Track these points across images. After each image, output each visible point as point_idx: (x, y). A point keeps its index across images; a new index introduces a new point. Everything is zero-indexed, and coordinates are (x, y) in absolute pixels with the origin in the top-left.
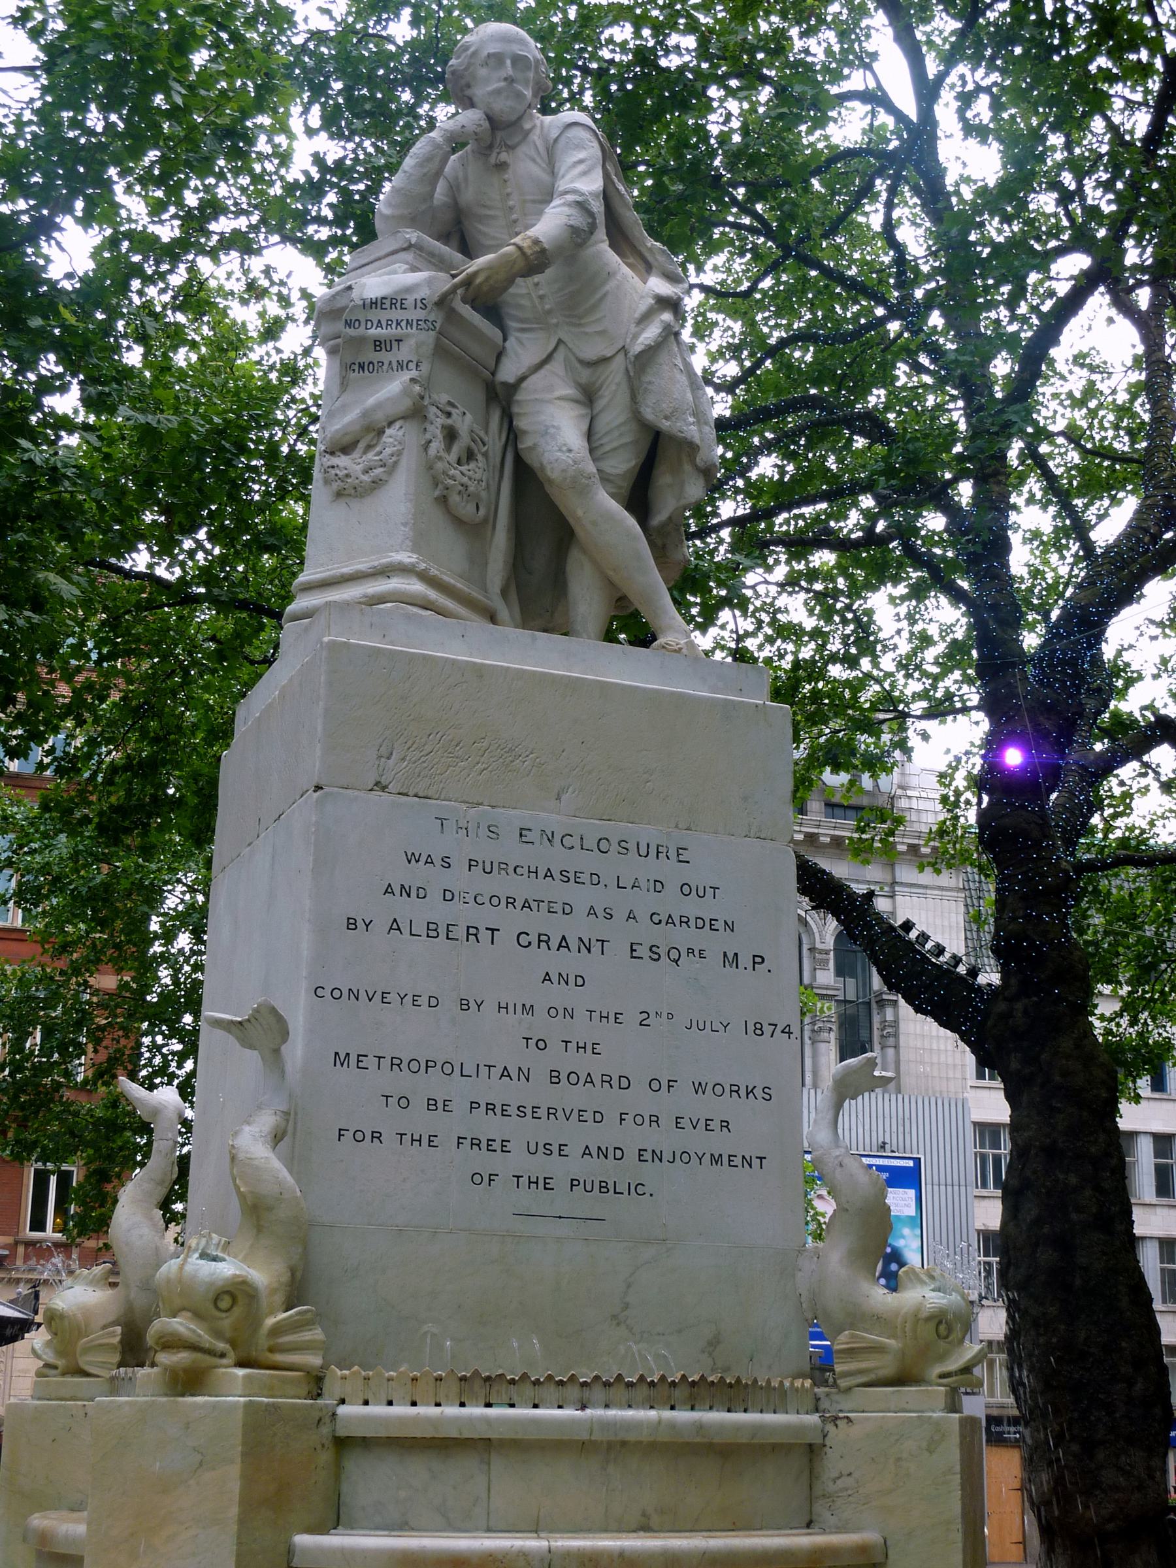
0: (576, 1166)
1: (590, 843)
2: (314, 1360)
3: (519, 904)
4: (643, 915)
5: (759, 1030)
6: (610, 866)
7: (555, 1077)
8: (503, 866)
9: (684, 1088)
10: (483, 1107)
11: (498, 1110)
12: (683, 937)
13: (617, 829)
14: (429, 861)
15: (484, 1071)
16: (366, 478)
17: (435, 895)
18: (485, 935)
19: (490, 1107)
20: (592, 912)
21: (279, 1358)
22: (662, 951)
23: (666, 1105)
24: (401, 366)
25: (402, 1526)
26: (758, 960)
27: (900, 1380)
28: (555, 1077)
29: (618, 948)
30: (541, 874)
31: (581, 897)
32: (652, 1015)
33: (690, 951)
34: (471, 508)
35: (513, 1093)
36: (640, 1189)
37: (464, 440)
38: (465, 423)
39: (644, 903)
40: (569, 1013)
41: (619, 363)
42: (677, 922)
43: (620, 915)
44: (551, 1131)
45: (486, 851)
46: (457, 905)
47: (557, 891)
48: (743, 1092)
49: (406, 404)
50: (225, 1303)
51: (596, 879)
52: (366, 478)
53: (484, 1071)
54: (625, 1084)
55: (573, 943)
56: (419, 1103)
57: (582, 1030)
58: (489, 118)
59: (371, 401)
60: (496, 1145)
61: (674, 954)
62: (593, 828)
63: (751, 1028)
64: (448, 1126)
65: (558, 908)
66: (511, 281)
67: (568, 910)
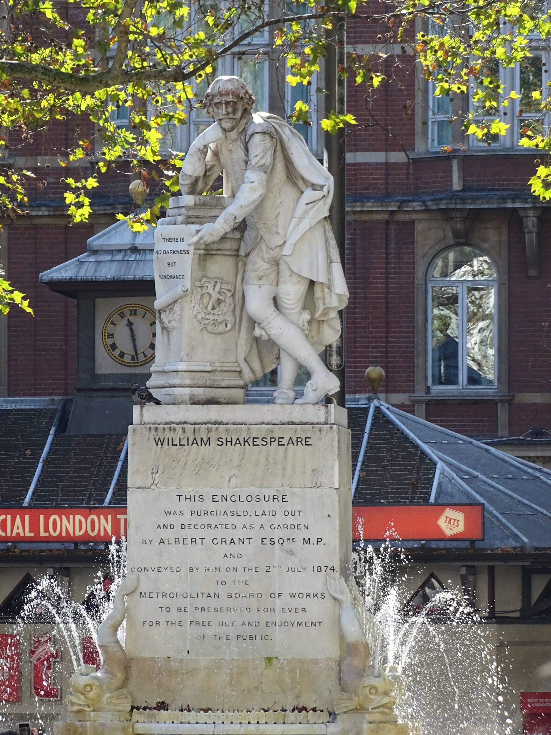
0: (239, 630)
3: (213, 527)
8: (206, 513)
9: (286, 597)
10: (200, 609)
11: (206, 610)
13: (255, 491)
15: (200, 595)
17: (178, 527)
19: (203, 609)
20: (245, 527)
22: (276, 540)
23: (279, 603)
26: (319, 540)
28: (230, 596)
30: (222, 513)
32: (271, 567)
33: (288, 539)
35: (213, 603)
36: (267, 638)
42: (282, 527)
43: (257, 527)
44: (227, 618)
45: (198, 506)
47: (230, 520)
48: (312, 596)
50: (88, 689)
53: (200, 595)
55: (236, 541)
56: (174, 610)
57: (241, 576)
60: (206, 624)
61: (281, 541)
63: (316, 569)
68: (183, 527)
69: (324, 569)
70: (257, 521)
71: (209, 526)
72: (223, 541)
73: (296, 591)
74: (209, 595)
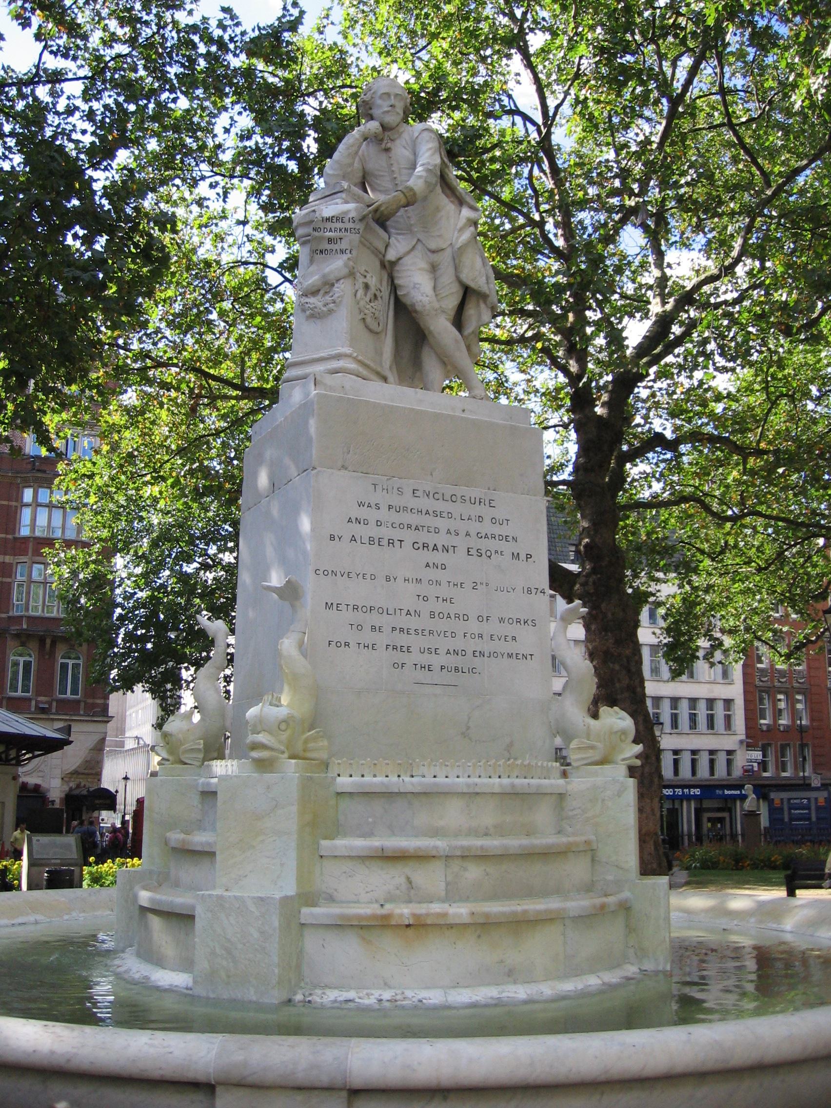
1: (447, 497)
2: (324, 755)
3: (413, 528)
4: (473, 533)
5: (529, 591)
6: (457, 509)
7: (432, 615)
8: (405, 509)
12: (493, 545)
13: (461, 490)
14: (369, 506)
16: (325, 309)
18: (397, 544)
19: (402, 630)
20: (449, 532)
21: (308, 755)
22: (483, 552)
24: (342, 252)
25: (369, 834)
26: (529, 556)
27: (602, 762)
28: (432, 615)
29: (462, 551)
31: (442, 524)
33: (496, 552)
34: (376, 324)
35: (413, 623)
37: (373, 290)
38: (373, 281)
39: (474, 527)
40: (438, 583)
41: (449, 252)
43: (462, 533)
45: (396, 500)
46: (383, 529)
49: (345, 271)
51: (450, 515)
52: (325, 309)
54: (466, 618)
55: (440, 547)
56: (367, 628)
57: (444, 591)
58: (382, 125)
59: (327, 270)
60: (404, 649)
61: (488, 553)
62: (449, 490)
64: (382, 639)
65: (432, 530)
66: (397, 210)
67: (437, 531)
68: (379, 524)
69: (534, 591)
70: (463, 527)
71: (409, 527)
72: (425, 546)
73: (506, 616)
74: (408, 613)
